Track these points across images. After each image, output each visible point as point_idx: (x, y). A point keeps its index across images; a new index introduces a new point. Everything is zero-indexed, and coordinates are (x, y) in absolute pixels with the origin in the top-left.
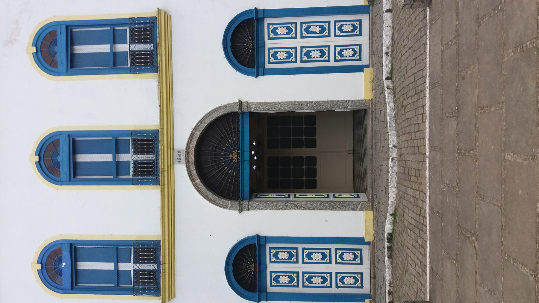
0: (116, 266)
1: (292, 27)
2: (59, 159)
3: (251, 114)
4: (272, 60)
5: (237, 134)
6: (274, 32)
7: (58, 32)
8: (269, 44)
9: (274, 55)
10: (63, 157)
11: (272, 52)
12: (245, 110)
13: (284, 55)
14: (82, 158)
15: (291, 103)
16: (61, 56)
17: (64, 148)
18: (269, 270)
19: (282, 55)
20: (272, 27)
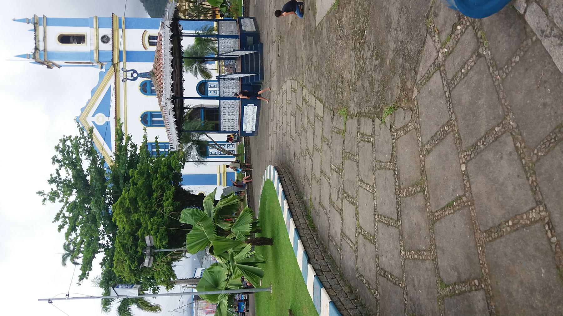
0: (165, 150)
1: (215, 85)
2: (147, 119)
3: (204, 108)
4: (210, 93)
5: (200, 113)
6: (210, 86)
7: (147, 83)
8: (209, 89)
9: (210, 92)
10: (149, 119)
11: (210, 91)
12: (202, 107)
13: (213, 92)
14: (154, 119)
15: (215, 105)
16: (148, 90)
17: (149, 116)
18: (209, 150)
19: (212, 92)
20: (210, 85)
